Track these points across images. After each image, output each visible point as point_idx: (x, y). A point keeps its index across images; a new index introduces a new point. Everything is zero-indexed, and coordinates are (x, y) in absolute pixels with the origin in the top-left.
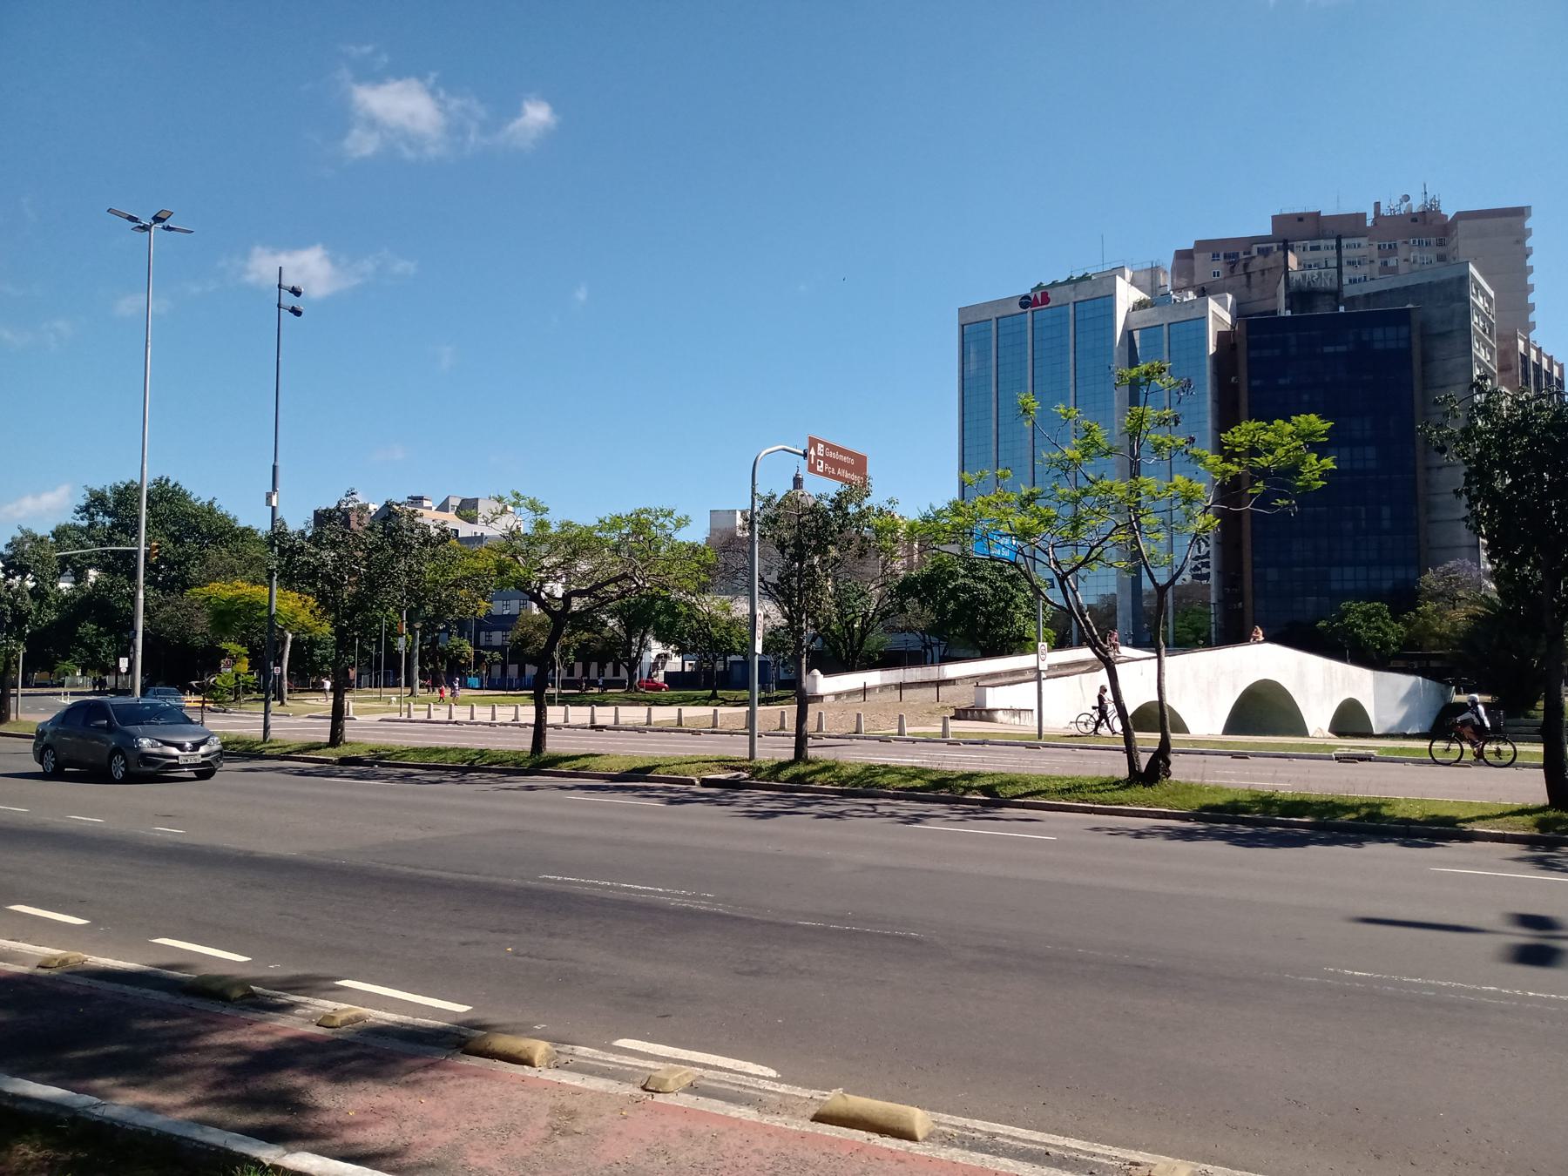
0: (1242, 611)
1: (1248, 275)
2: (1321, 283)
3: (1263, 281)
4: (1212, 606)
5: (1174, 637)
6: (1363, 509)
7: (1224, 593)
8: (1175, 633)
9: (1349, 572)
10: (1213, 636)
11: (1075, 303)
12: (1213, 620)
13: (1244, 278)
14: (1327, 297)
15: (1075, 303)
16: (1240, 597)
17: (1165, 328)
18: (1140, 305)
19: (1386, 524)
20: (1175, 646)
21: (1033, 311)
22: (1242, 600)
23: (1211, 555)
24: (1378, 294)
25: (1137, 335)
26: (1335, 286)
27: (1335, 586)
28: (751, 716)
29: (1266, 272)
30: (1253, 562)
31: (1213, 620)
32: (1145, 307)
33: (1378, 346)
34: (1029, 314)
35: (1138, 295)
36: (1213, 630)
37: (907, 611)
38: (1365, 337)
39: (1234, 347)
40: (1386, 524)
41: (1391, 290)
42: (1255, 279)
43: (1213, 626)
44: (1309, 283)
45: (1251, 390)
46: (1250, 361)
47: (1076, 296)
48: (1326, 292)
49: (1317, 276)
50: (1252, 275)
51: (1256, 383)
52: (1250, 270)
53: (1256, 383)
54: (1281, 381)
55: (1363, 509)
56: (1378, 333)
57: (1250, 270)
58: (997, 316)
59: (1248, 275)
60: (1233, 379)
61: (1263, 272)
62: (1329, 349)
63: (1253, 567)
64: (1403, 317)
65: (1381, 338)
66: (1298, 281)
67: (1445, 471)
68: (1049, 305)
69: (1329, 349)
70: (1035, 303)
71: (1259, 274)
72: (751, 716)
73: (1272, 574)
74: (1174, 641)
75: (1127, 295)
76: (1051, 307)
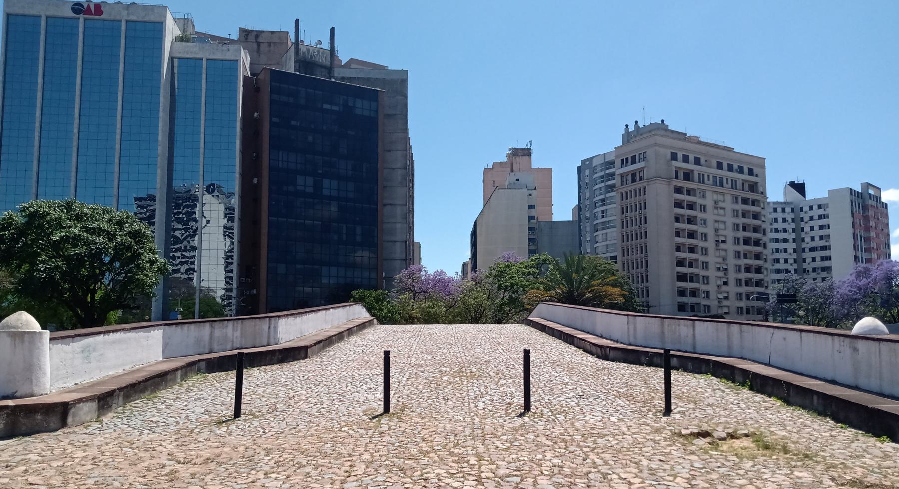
1: (259, 44)
2: (319, 59)
3: (270, 51)
6: (344, 226)
9: (333, 270)
11: (127, 22)
13: (255, 46)
14: (323, 70)
15: (127, 22)
16: (255, 284)
17: (204, 62)
18: (181, 39)
19: (358, 238)
21: (85, 20)
23: (235, 250)
24: (351, 79)
25: (176, 62)
26: (328, 64)
29: (272, 45)
32: (188, 41)
33: (358, 112)
34: (82, 20)
35: (178, 33)
37: (144, 235)
38: (350, 104)
39: (257, 90)
40: (358, 238)
41: (358, 78)
42: (264, 48)
44: (311, 56)
45: (272, 125)
46: (272, 102)
47: (128, 15)
48: (322, 67)
49: (316, 53)
50: (261, 44)
51: (275, 120)
52: (260, 40)
53: (275, 120)
54: (293, 123)
55: (344, 226)
56: (359, 103)
57: (260, 40)
58: (48, 14)
59: (259, 44)
60: (256, 115)
61: (269, 44)
62: (326, 106)
64: (373, 96)
65: (361, 107)
66: (304, 53)
67: (388, 207)
68: (102, 17)
69: (326, 106)
70: (88, 11)
71: (266, 45)
73: (281, 268)
75: (172, 31)
76: (104, 20)
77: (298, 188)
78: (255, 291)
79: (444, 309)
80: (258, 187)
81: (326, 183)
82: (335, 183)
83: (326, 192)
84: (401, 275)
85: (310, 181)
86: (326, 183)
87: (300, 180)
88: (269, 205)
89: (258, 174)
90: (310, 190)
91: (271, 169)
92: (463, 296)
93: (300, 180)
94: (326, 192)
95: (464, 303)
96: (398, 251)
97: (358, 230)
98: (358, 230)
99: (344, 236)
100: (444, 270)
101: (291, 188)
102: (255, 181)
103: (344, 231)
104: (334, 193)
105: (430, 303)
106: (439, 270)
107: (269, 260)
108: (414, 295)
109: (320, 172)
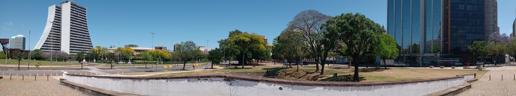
0: (448, 44)
4: (441, 42)
5: (433, 50)
7: (444, 40)
8: (433, 49)
9: (470, 34)
10: (441, 50)
12: (441, 46)
16: (447, 40)
19: (478, 24)
20: (433, 53)
22: (448, 41)
23: (441, 30)
27: (468, 38)
28: (298, 66)
30: (451, 32)
31: (441, 46)
36: (441, 49)
40: (478, 24)
43: (441, 48)
63: (451, 33)
72: (298, 66)
73: (455, 35)
74: (433, 52)
77: (460, 8)
78: (447, 42)
79: (506, 48)
80: (448, 9)
81: (468, 6)
82: (471, 6)
83: (468, 9)
84: (491, 36)
85: (463, 6)
86: (468, 6)
87: (460, 6)
88: (451, 14)
89: (448, 6)
90: (463, 9)
91: (451, 3)
92: (512, 42)
93: (460, 6)
94: (468, 9)
95: (512, 45)
96: (491, 28)
97: (478, 21)
98: (478, 21)
99: (474, 24)
100: (506, 33)
101: (457, 9)
102: (447, 7)
103: (474, 22)
104: (471, 9)
105: (501, 45)
106: (504, 33)
107: (451, 32)
108: (496, 42)
109: (466, 3)
